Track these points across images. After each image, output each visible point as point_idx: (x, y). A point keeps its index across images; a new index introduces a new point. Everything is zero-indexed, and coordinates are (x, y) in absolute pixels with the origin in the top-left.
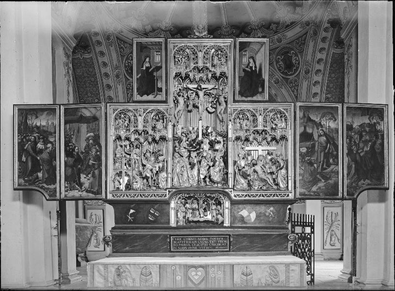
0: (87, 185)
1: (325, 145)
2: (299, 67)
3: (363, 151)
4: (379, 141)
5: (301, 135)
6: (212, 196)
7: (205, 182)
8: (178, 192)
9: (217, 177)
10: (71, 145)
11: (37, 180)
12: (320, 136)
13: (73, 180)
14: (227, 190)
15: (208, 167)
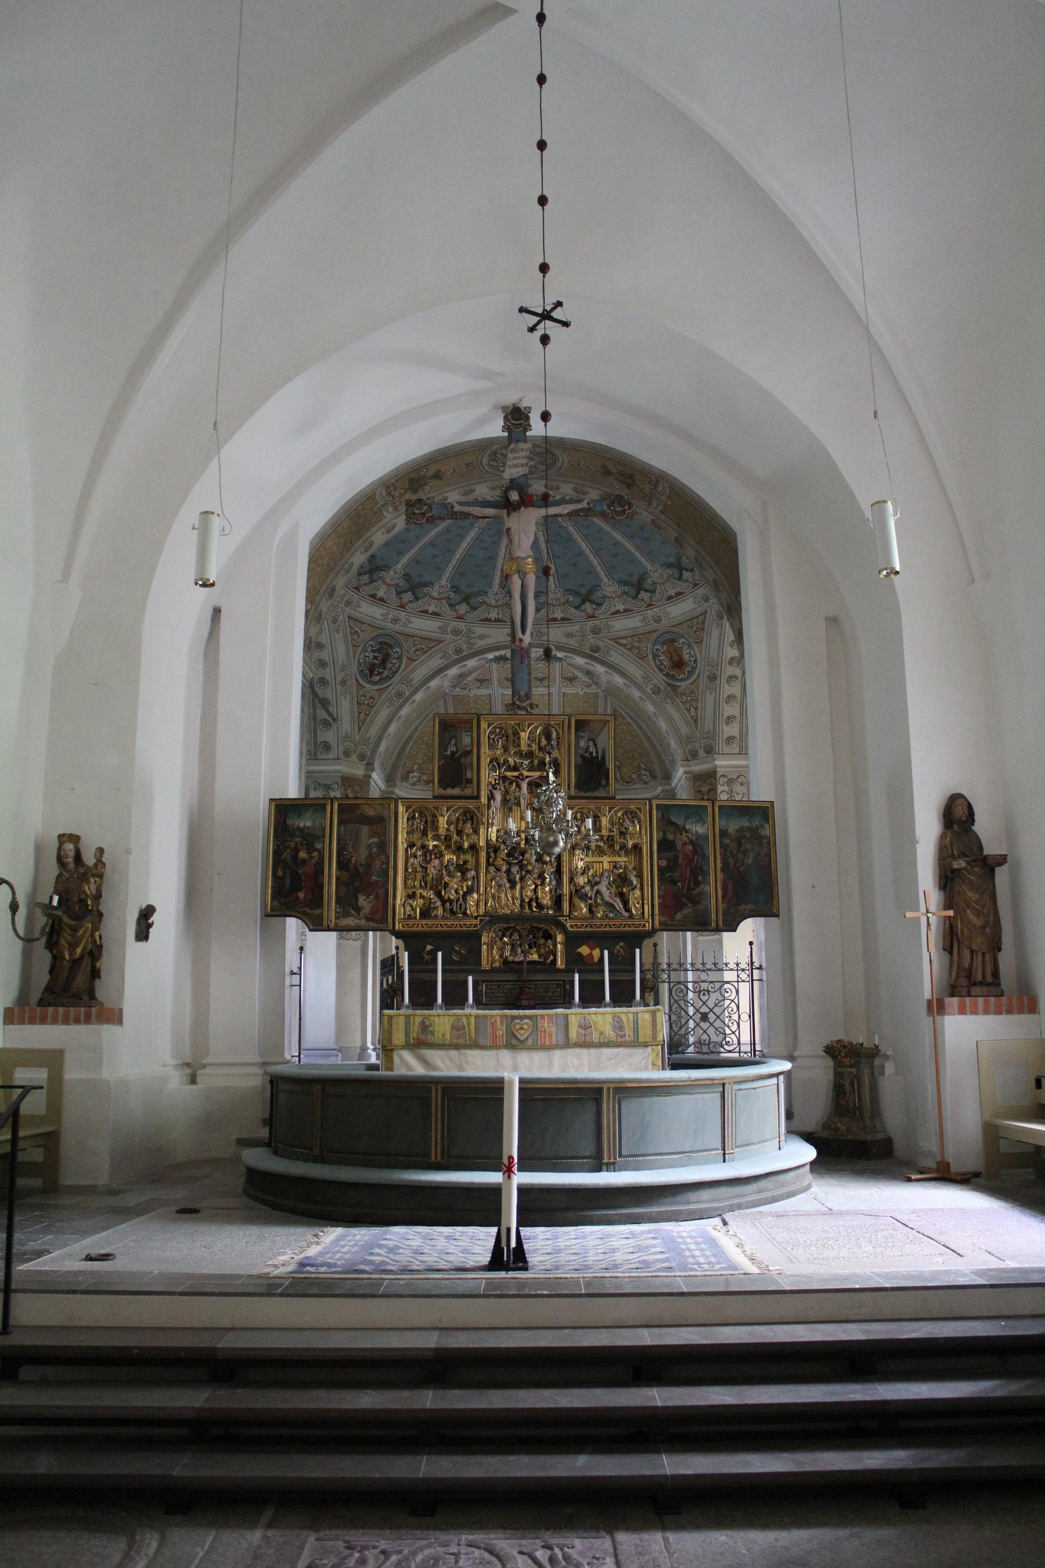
1: (691, 857)
2: (696, 667)
3: (743, 865)
4: (764, 851)
5: (658, 843)
6: (540, 926)
7: (530, 907)
8: (492, 919)
9: (546, 901)
10: (347, 854)
11: (296, 903)
12: (684, 844)
13: (347, 903)
14: (560, 918)
15: (534, 886)
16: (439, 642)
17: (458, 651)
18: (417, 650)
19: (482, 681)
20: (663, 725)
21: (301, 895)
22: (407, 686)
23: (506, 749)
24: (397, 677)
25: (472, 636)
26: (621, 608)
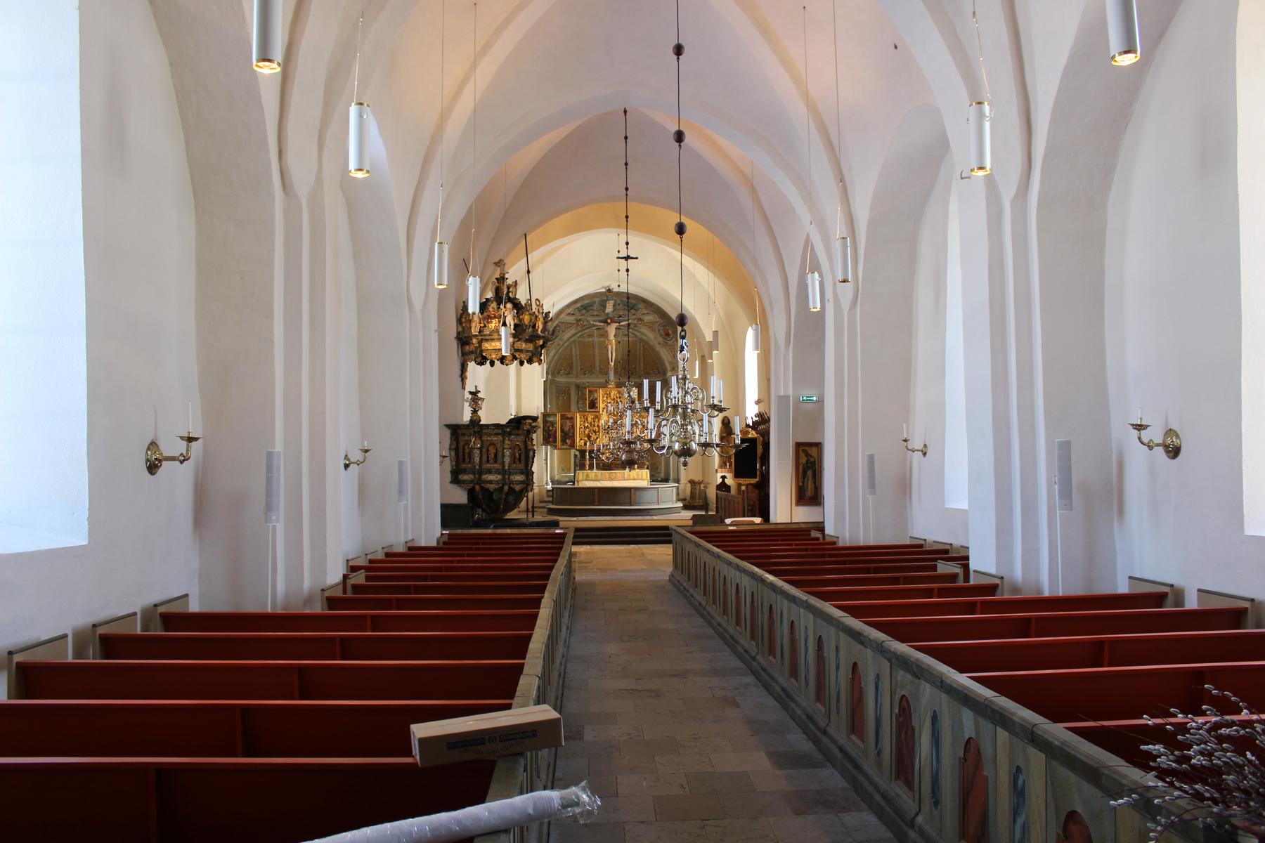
0: (569, 444)
13: (564, 441)
19: (590, 336)
20: (664, 357)
21: (551, 439)
23: (607, 397)
24: (557, 339)
26: (645, 312)
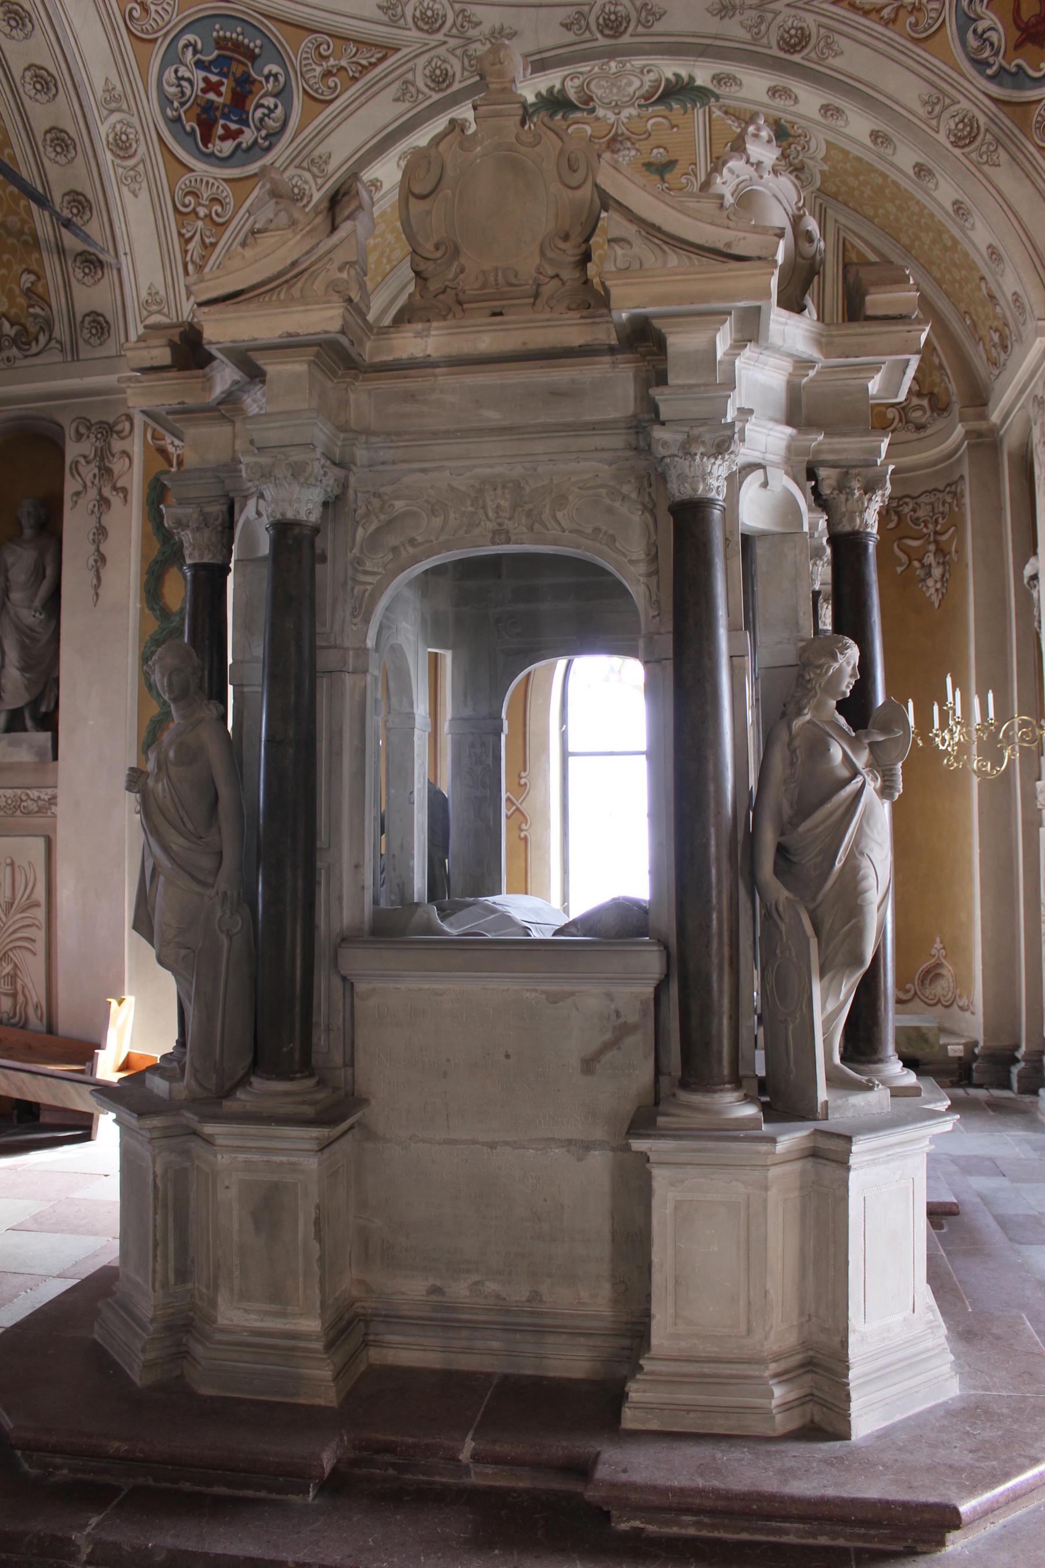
16: (389, 50)
17: (440, 79)
18: (328, 74)
22: (315, 176)
25: (472, 33)
